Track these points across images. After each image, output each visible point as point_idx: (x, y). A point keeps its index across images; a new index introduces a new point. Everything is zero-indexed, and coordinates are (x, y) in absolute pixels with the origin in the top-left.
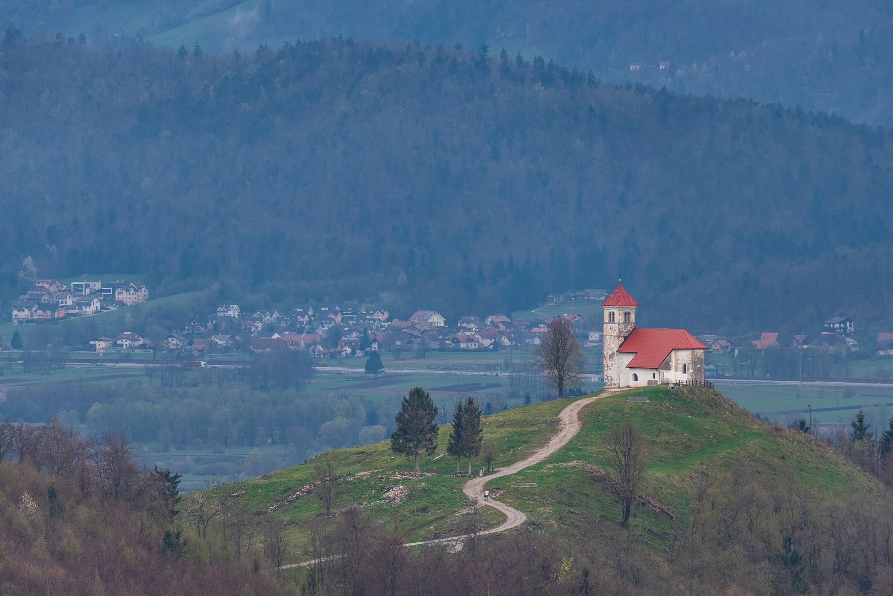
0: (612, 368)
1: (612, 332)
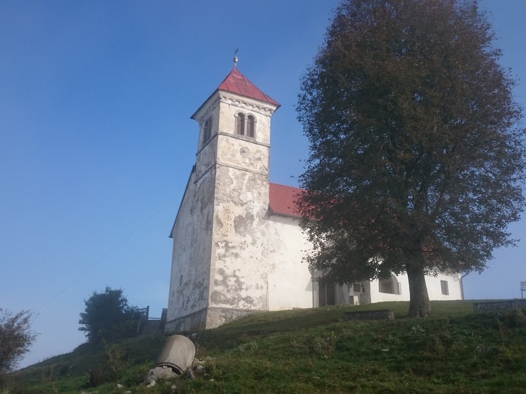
1: (247, 161)
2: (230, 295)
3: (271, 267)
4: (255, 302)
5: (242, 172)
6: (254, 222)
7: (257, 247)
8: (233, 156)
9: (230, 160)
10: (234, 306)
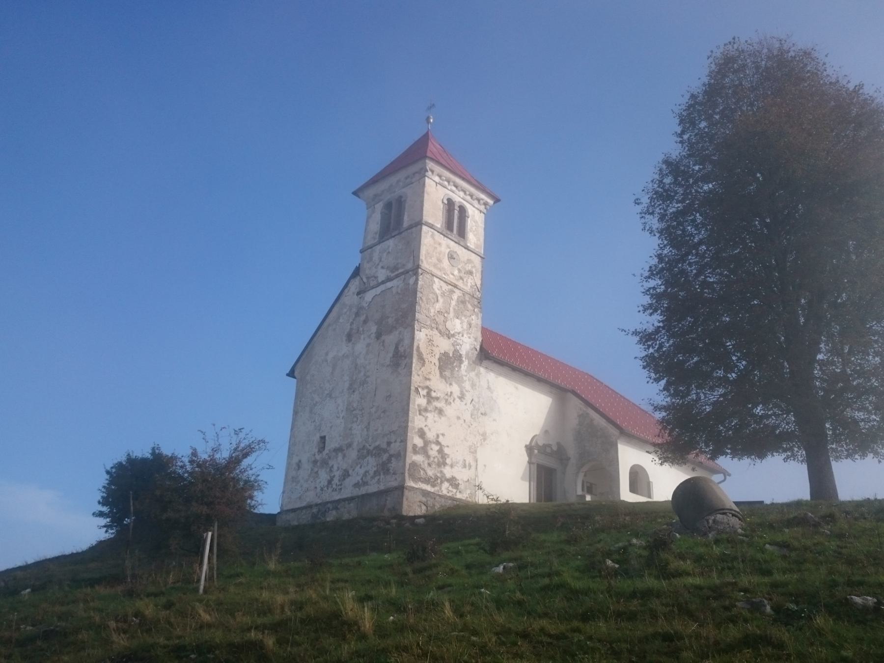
0: (450, 411)
1: (456, 272)
2: (431, 470)
3: (482, 438)
4: (462, 487)
5: (450, 287)
6: (462, 366)
7: (466, 404)
8: (439, 260)
9: (435, 266)
10: (437, 488)
